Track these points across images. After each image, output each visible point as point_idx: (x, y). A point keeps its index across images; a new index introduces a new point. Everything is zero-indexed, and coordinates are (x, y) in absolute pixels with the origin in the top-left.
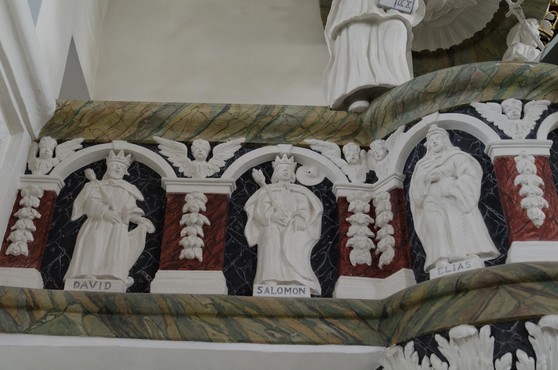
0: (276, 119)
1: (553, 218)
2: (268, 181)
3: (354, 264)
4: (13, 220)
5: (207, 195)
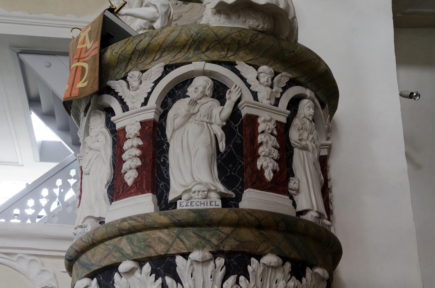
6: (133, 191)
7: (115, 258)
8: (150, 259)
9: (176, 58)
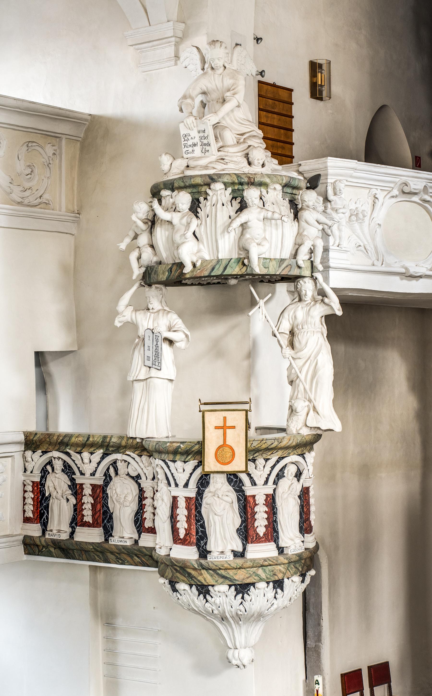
0: (110, 444)
1: (188, 534)
2: (117, 474)
3: (147, 527)
4: (24, 498)
5: (91, 485)
6: (263, 539)
7: (255, 579)
8: (275, 582)
9: (284, 453)
